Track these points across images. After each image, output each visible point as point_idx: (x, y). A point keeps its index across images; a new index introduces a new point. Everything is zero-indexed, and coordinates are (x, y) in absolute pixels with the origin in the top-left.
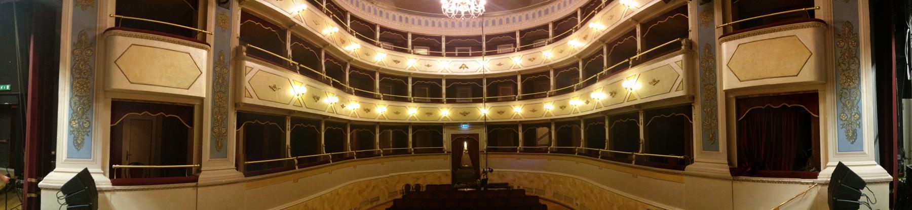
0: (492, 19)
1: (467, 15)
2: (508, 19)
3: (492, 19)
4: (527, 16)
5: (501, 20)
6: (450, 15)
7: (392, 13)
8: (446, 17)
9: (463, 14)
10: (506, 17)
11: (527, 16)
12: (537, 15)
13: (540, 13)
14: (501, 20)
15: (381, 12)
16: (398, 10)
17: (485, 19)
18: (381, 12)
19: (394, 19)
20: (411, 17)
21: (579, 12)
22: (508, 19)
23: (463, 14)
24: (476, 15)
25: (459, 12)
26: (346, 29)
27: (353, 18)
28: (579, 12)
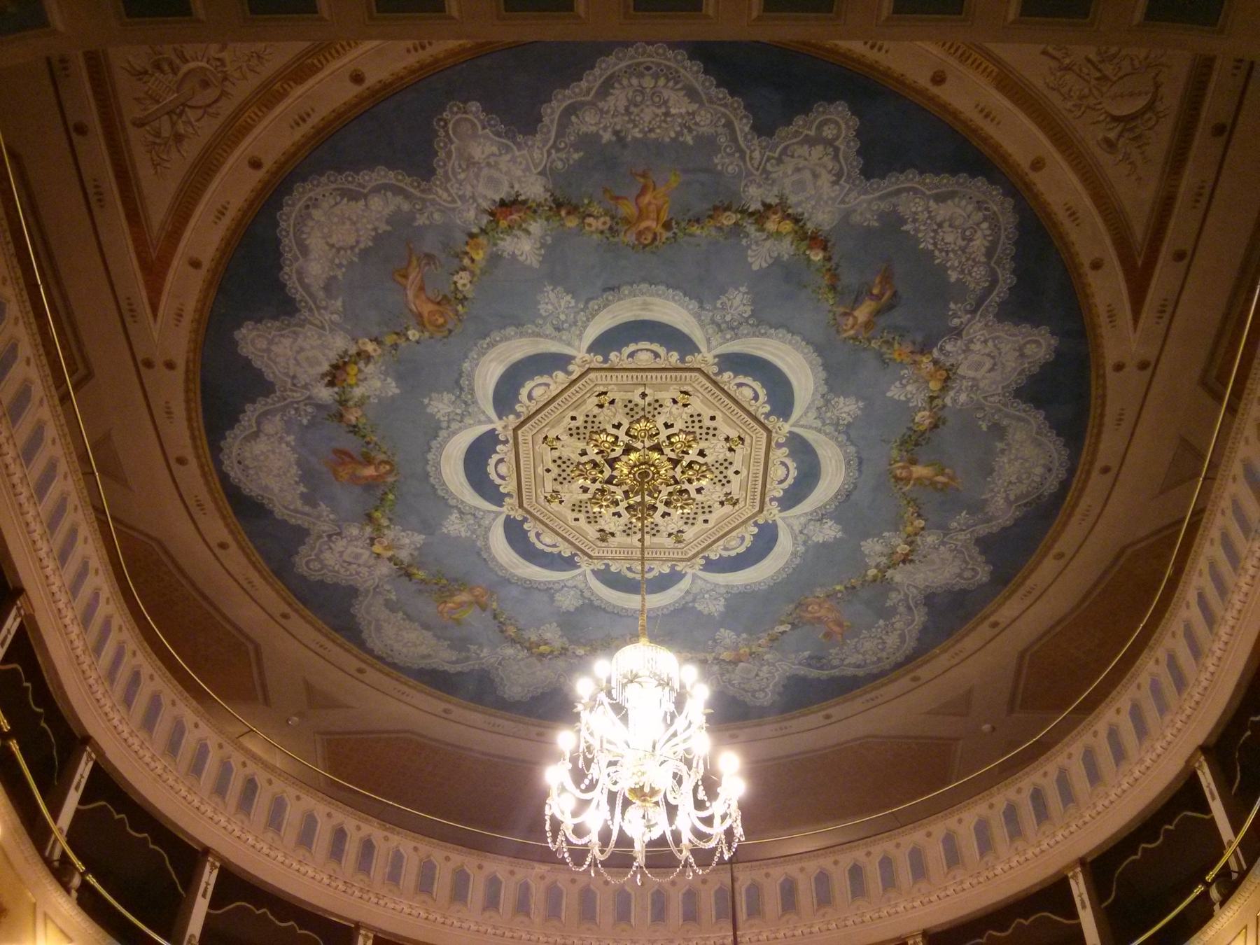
0: (778, 873)
1: (661, 855)
2: (856, 872)
3: (778, 873)
4: (950, 841)
5: (823, 879)
6: (579, 854)
7: (301, 804)
8: (549, 857)
9: (639, 849)
10: (847, 859)
11: (950, 841)
12: (999, 831)
13: (1011, 814)
14: (823, 879)
15: (250, 787)
16: (334, 793)
17: (745, 877)
18: (250, 787)
19: (306, 838)
20: (389, 841)
21: (1206, 779)
22: (856, 872)
23: (639, 849)
24: (703, 857)
25: (625, 841)
26: (36, 831)
27: (105, 784)
28: (1206, 779)
